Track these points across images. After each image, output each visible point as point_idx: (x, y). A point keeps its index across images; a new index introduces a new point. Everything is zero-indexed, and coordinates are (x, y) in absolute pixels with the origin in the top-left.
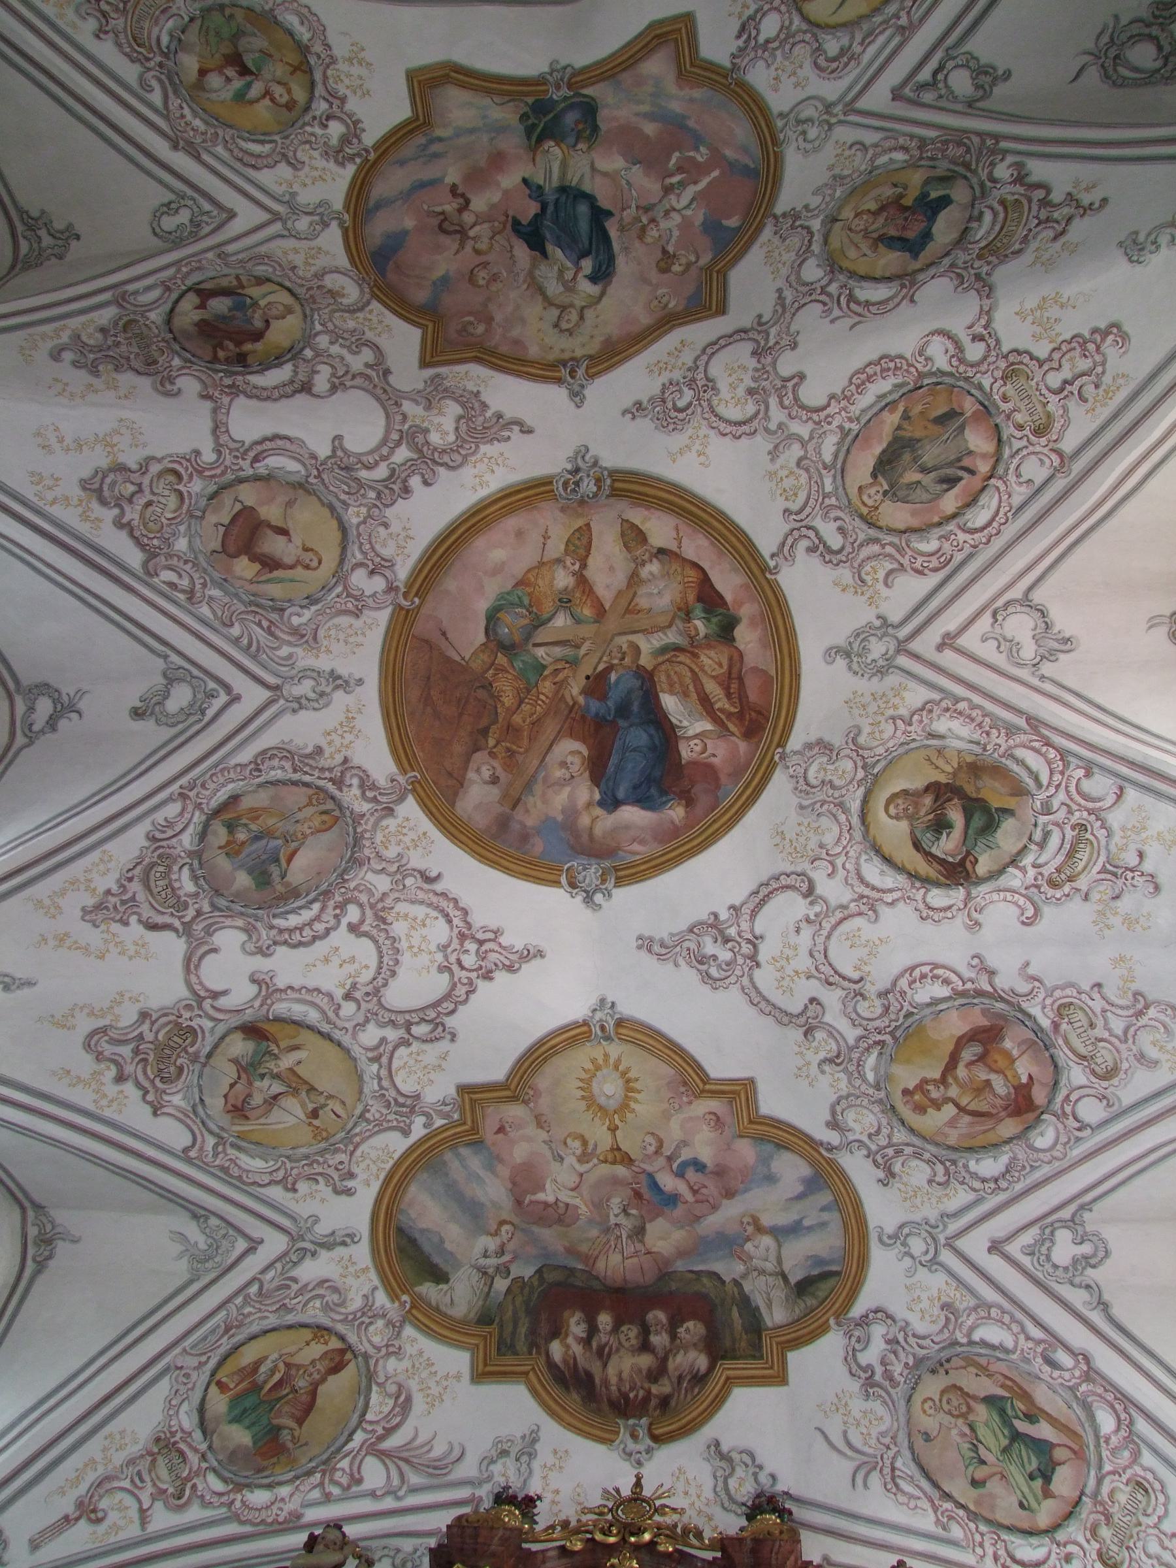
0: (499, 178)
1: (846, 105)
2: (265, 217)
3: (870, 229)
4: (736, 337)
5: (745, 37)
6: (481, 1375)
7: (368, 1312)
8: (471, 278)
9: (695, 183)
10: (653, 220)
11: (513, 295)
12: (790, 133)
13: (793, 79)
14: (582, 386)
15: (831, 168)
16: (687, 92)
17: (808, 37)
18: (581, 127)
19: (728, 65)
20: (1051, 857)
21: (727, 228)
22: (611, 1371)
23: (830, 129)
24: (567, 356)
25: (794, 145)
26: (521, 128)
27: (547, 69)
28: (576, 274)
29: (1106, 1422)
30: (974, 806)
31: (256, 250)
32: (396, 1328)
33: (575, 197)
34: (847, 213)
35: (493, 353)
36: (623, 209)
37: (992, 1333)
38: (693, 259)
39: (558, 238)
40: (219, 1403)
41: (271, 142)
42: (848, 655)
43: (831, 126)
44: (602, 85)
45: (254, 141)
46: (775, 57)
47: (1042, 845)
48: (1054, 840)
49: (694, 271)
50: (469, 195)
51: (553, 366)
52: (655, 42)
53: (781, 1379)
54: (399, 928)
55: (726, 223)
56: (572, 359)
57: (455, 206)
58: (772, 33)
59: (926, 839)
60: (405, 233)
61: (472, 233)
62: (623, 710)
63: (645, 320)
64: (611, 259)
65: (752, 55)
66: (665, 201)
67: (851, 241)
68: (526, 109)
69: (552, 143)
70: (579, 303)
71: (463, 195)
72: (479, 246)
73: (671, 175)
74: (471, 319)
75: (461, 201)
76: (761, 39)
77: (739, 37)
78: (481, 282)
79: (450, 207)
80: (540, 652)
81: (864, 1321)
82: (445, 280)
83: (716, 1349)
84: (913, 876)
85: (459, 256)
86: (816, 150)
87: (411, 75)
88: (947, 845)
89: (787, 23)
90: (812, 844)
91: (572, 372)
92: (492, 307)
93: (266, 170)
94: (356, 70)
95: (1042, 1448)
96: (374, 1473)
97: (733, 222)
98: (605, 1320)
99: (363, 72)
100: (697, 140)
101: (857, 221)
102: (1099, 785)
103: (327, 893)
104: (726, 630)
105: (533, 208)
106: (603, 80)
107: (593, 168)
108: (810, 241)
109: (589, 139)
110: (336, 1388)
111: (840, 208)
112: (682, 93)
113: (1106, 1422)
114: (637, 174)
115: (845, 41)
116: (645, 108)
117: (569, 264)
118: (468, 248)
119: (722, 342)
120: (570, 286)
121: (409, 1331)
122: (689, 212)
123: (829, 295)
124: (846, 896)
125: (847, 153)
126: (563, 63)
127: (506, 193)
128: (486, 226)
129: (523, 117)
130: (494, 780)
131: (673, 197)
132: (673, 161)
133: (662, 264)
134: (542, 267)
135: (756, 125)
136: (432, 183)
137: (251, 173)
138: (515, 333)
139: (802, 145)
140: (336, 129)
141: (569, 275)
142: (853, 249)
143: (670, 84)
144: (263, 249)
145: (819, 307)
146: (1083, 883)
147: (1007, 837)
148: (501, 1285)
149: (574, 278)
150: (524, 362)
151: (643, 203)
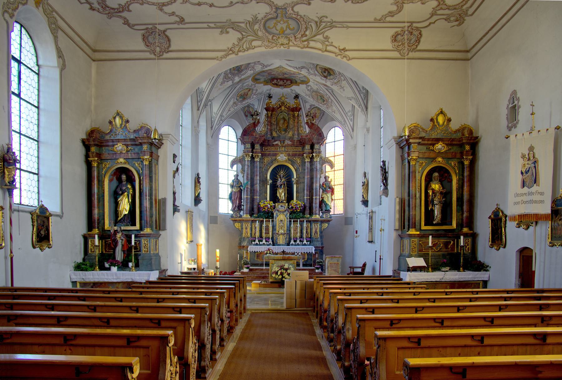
6: (264, 85)
7: (252, 85)
20: (336, 81)
22: (279, 83)
29: (330, 100)
30: (329, 72)
32: (255, 85)
37: (321, 92)
40: (238, 98)
47: (335, 79)
48: (336, 80)
53: (299, 86)
54: (255, 68)
59: (323, 73)
81: (308, 85)
83: (291, 83)
84: (321, 75)
88: (325, 74)
90: (310, 66)
95: (324, 100)
96: (255, 96)
98: (279, 80)
102: (342, 78)
103: (247, 68)
110: (250, 93)
113: (330, 100)
121: (256, 84)
124: (313, 73)
146: (338, 85)
147: (331, 77)
148: (266, 79)
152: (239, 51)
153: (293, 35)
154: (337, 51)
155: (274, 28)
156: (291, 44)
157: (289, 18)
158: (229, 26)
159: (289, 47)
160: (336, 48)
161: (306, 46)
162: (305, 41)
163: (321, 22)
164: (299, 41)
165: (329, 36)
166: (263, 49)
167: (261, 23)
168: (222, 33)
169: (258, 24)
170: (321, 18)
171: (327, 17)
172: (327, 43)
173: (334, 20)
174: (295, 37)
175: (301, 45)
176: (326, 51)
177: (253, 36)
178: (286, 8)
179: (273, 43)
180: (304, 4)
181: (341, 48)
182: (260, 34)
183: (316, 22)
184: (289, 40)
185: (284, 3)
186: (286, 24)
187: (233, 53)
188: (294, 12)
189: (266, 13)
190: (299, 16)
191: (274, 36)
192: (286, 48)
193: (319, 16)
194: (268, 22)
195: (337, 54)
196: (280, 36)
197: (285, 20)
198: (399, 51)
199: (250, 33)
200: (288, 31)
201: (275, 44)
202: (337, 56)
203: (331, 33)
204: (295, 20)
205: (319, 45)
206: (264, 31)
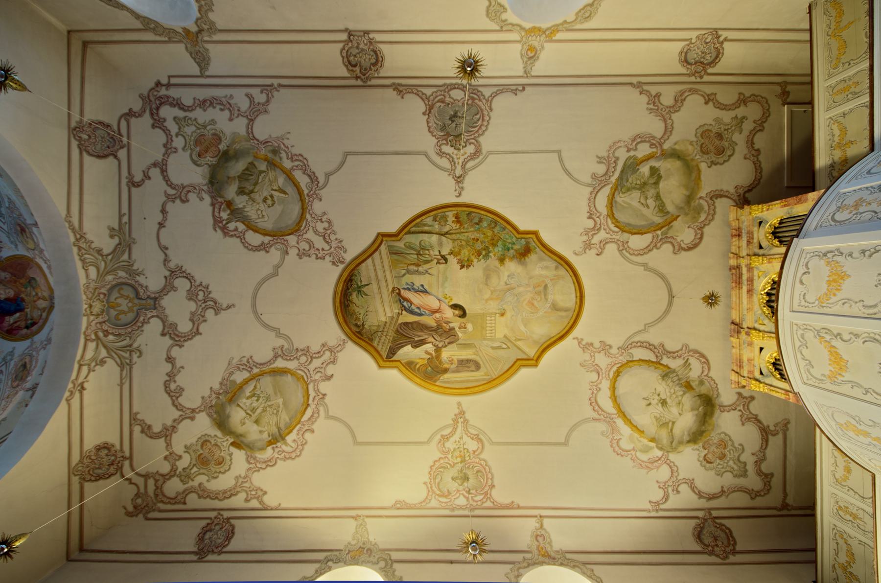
42: (12, 352)
62: (18, 305)
80: (29, 289)
104: (27, 327)
130: (6, 278)
152: (80, 248)
153: (107, 318)
154: (80, 380)
155: (119, 295)
156: (92, 318)
157: (138, 313)
158: (124, 241)
159: (87, 315)
160: (86, 378)
161: (88, 338)
162: (96, 334)
163: (131, 351)
164: (95, 328)
165: (106, 365)
166: (83, 280)
167: (128, 279)
168: (112, 229)
169: (127, 276)
170: (138, 350)
171: (139, 357)
172: (93, 364)
173: (134, 366)
174: (104, 322)
175: (89, 331)
176: (81, 366)
177: (105, 268)
178: (155, 308)
179: (93, 294)
180: (164, 329)
181: (86, 385)
182: (110, 278)
183: (130, 346)
184: (98, 315)
185: (164, 306)
186: (126, 309)
187: (77, 240)
188: (149, 318)
189: (146, 287)
190: (141, 325)
191: (105, 295)
192: (84, 312)
193: (143, 348)
194: (130, 289)
195: (75, 382)
196: (105, 303)
197: (135, 309)
198: (81, 461)
199: (111, 265)
200: (113, 313)
201: (92, 297)
202: (73, 382)
203: (111, 366)
204: (134, 320)
205: (89, 354)
206: (114, 283)
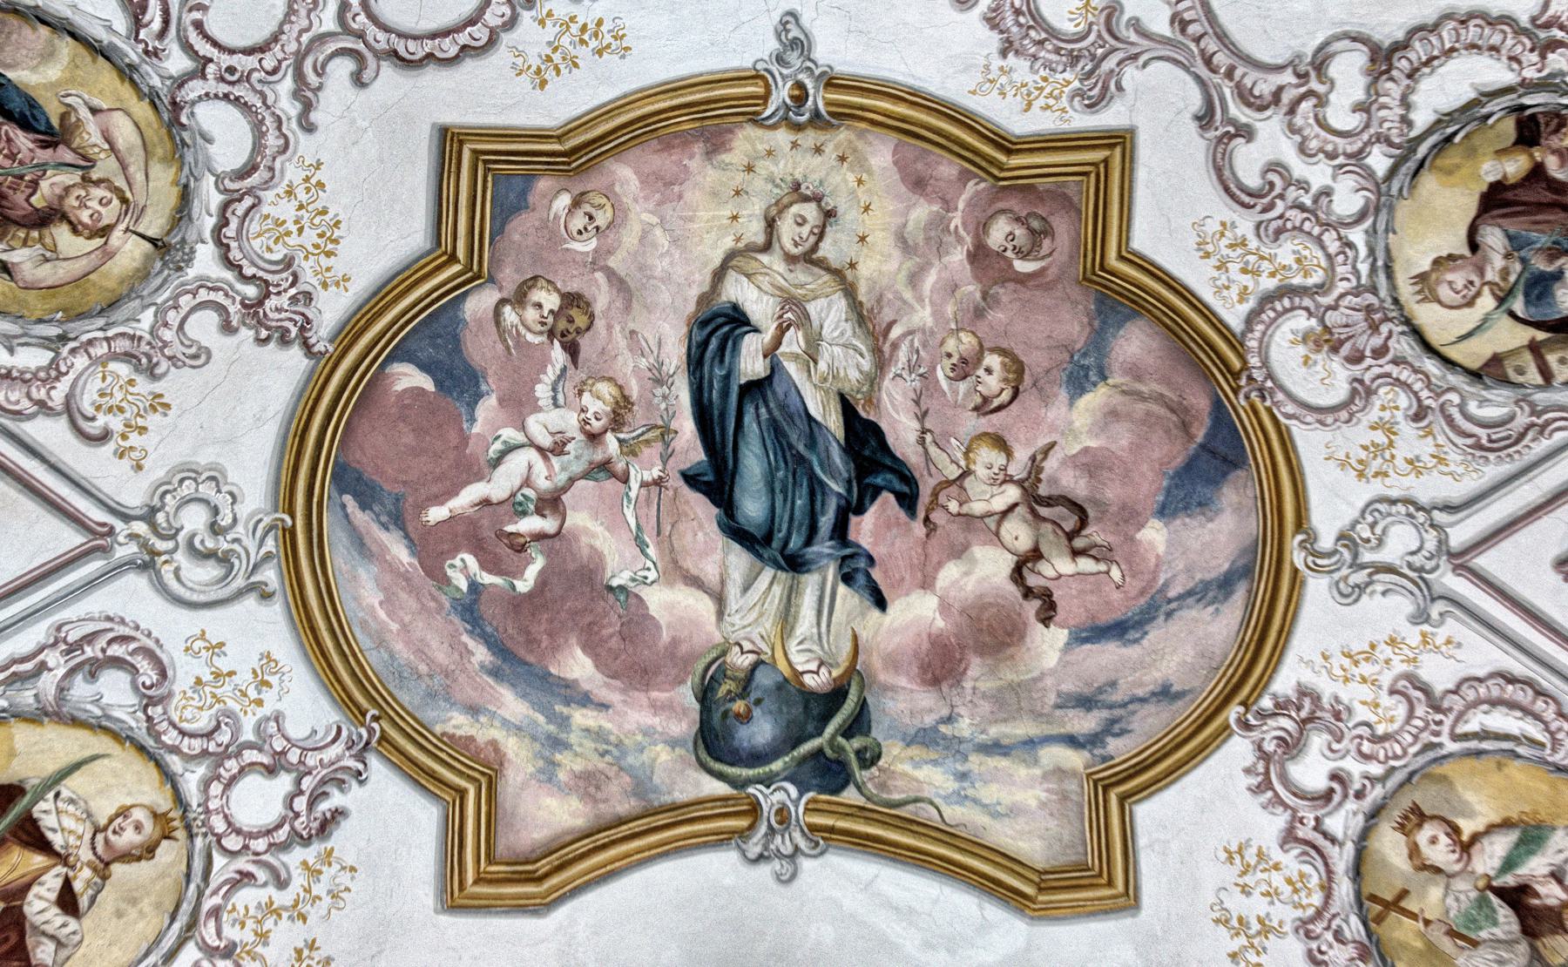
0: (940, 623)
1: (105, 550)
2: (1485, 561)
3: (73, 177)
4: (417, 50)
5: (324, 806)
8: (1016, 368)
9: (486, 502)
10: (594, 438)
11: (923, 316)
12: (252, 546)
13: (223, 664)
14: (780, 60)
15: (159, 404)
16: (483, 732)
17: (170, 737)
18: (739, 706)
19: (373, 761)
21: (425, 367)
23: (153, 511)
24: (810, 138)
25: (243, 510)
26: (877, 733)
27: (806, 864)
28: (777, 342)
31: (1507, 468)
33: (768, 539)
34: (129, 252)
35: (976, 163)
36: (658, 483)
38: (509, 315)
39: (812, 443)
41: (1466, 737)
43: (149, 515)
44: (680, 796)
45: (1507, 737)
46: (258, 729)
49: (510, 277)
50: (1012, 590)
51: (842, 115)
52: (543, 866)
55: (426, 382)
56: (798, 128)
57: (1045, 568)
58: (253, 781)
60: (1163, 512)
61: (1012, 493)
63: (624, 175)
64: (695, 362)
65: (312, 760)
66: (562, 478)
67: (124, 167)
68: (861, 775)
69: (809, 680)
70: (773, 261)
71: (1028, 593)
72: (998, 459)
73: (540, 537)
74: (1022, 266)
75: (1032, 581)
76: (285, 782)
77: (338, 814)
78: (993, 360)
79: (1057, 566)
82: (1078, 383)
85: (1042, 442)
86: (190, 472)
87: (1129, 901)
89: (216, 789)
91: (800, 96)
92: (972, 290)
93: (1481, 673)
94: (1255, 907)
97: (409, 378)
99: (1237, 904)
100: (471, 607)
101: (109, 214)
105: (864, 528)
106: (674, 807)
107: (720, 600)
108: (223, 222)
109: (723, 672)
111: (143, 274)
112: (497, 734)
114: (621, 564)
115: (81, 690)
116: (582, 718)
117: (792, 368)
118: (1022, 455)
119: (449, 47)
120: (794, 309)
122: (510, 434)
123: (188, 48)
125: (116, 423)
126: (765, 871)
127: (927, 584)
128: (977, 508)
129: (869, 758)
131: (543, 484)
132: (532, 572)
133: (581, 321)
134: (854, 375)
135: (327, 594)
136: (1095, 633)
137: (1518, 665)
138: (922, 211)
139: (223, 501)
140: (1311, 771)
141: (794, 342)
142: (121, 144)
143: (519, 757)
144: (1494, 470)
145: (213, 28)
149: (782, 330)
150: (904, 130)
151: (611, 485)
